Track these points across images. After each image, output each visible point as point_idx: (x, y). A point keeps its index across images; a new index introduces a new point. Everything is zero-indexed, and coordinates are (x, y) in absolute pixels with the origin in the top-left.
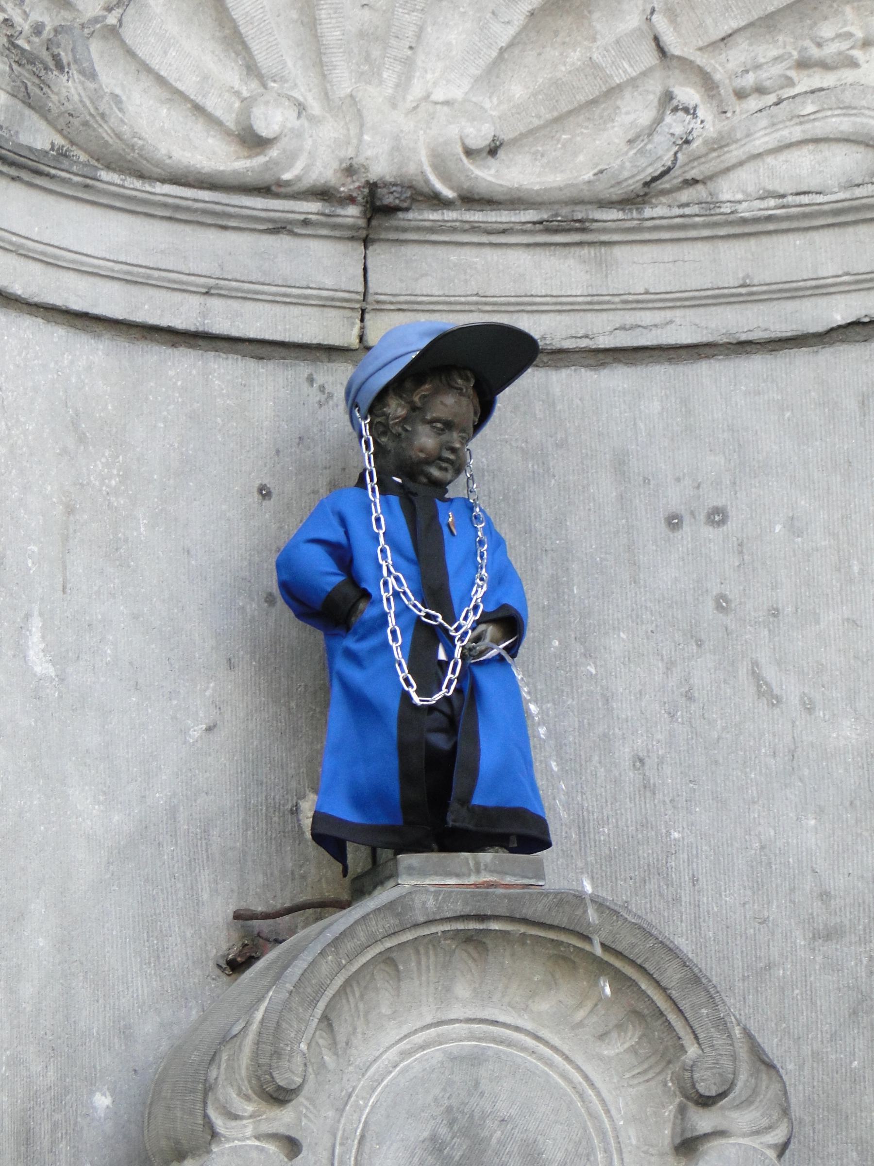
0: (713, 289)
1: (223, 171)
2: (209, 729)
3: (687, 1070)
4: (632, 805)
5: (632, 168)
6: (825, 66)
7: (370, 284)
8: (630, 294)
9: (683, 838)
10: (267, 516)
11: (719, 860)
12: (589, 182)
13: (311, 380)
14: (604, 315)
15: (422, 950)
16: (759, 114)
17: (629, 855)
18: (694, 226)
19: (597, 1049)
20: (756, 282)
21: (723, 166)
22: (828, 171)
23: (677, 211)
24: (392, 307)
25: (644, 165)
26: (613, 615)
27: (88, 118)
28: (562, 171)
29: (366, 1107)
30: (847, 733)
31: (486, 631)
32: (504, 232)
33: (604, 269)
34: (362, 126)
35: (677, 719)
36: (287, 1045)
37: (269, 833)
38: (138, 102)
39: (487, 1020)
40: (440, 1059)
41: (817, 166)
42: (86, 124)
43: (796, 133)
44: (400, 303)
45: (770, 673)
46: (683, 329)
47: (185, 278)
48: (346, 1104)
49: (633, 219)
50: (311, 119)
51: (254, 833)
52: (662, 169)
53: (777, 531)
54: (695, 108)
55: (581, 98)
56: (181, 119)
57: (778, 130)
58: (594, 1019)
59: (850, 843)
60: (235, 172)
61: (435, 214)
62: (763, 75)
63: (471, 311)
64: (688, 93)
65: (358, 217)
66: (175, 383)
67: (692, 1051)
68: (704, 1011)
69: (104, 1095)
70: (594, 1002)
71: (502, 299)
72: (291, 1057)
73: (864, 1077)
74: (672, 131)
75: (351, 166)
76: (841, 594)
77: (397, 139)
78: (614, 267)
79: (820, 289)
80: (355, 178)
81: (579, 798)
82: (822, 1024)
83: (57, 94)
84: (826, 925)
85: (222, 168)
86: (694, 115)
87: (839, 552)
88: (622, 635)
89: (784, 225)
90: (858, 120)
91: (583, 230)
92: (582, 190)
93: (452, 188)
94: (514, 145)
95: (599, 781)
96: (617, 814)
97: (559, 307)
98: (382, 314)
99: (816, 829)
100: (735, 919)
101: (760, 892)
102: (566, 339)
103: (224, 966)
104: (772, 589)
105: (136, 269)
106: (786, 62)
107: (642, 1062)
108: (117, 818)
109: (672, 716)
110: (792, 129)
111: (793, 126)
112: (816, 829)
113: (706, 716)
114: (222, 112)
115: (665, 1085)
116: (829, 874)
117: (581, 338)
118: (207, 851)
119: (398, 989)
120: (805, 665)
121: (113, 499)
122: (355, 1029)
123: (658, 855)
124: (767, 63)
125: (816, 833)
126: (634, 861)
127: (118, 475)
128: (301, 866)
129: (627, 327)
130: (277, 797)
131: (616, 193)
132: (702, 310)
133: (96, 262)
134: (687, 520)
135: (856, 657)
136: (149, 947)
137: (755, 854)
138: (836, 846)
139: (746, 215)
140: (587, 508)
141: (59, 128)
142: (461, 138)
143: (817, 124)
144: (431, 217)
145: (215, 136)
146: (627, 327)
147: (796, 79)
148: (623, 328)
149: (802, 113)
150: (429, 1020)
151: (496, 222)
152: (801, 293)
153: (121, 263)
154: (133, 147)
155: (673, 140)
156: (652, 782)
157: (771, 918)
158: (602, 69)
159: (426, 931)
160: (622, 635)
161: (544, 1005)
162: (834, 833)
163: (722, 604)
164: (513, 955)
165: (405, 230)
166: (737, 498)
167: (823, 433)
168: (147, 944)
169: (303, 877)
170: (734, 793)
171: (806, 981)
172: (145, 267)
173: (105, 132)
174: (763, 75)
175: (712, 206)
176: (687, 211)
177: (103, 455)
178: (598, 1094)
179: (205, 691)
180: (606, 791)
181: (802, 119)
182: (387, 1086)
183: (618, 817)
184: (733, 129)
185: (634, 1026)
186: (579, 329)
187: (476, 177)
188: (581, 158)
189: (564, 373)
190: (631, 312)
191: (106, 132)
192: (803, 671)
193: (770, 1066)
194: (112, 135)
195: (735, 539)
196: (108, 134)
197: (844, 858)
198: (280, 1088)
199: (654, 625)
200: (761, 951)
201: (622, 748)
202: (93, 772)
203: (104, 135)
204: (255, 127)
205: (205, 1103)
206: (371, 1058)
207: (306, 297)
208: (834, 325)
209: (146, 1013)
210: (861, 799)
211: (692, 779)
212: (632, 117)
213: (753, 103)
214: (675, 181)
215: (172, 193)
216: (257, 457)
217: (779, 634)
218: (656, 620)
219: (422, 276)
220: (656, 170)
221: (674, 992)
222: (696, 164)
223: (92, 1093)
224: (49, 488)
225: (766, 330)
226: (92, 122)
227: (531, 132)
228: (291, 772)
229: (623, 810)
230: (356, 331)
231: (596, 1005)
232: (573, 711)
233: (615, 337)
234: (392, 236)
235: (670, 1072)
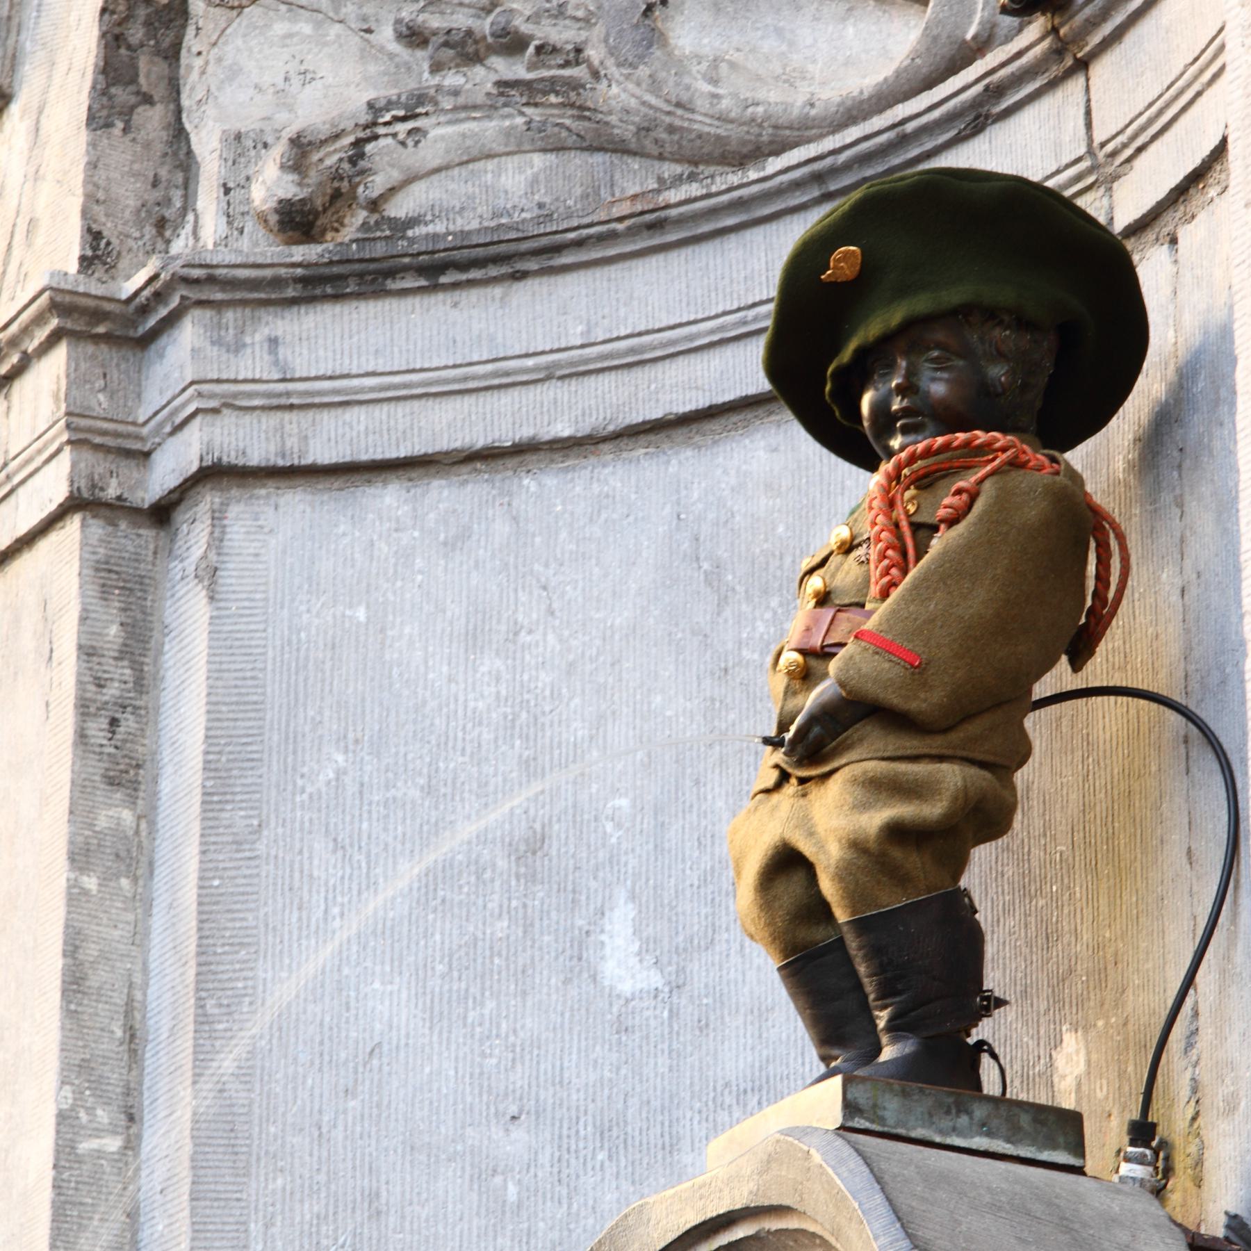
27: (668, 119)
38: (809, 41)
42: (671, 129)
56: (873, 28)
83: (610, 113)
141: (656, 153)
153: (754, 305)
173: (702, 124)
177: (768, 607)
203: (707, 129)
224: (659, 698)
226: (678, 122)
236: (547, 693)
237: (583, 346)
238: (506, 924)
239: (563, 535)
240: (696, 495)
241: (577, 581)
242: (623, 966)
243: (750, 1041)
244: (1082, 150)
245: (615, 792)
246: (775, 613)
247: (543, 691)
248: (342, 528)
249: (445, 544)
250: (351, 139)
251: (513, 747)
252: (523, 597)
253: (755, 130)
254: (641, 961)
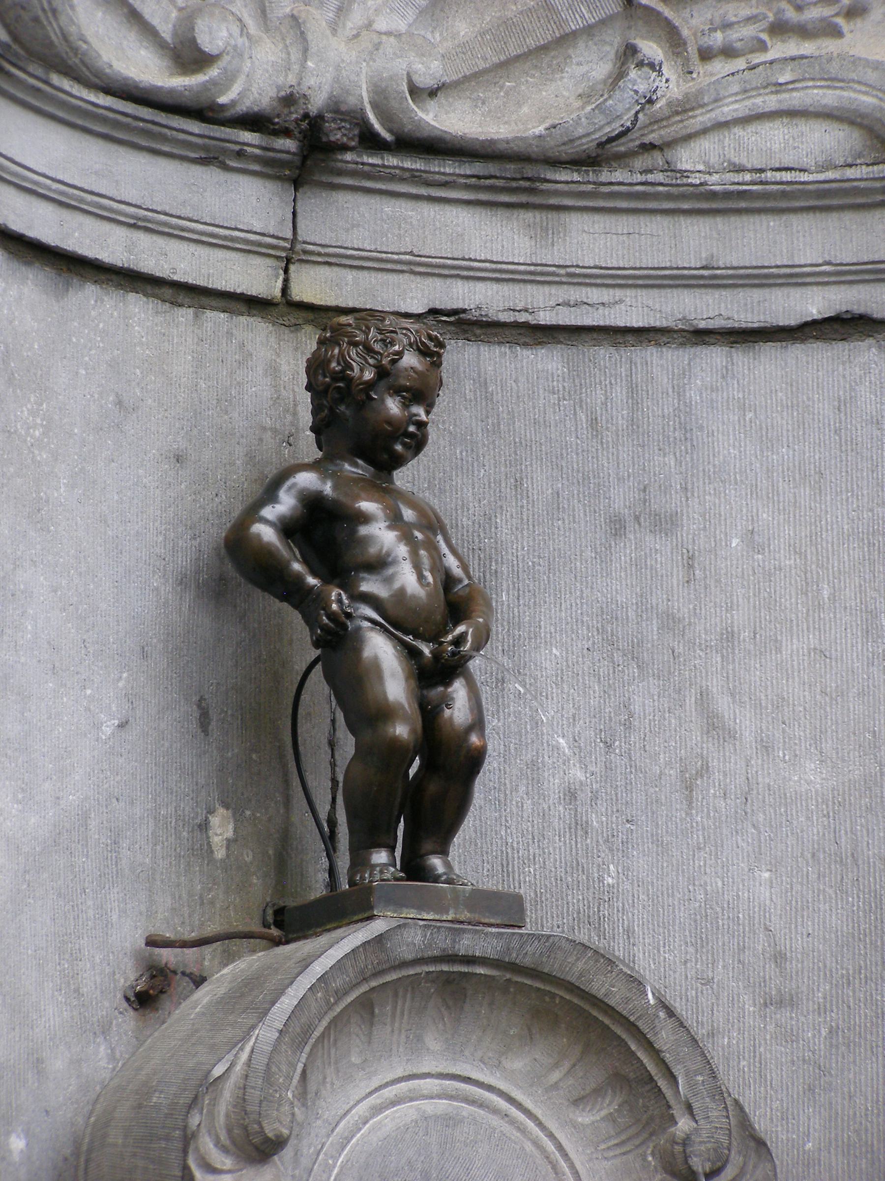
0: (671, 268)
1: (162, 87)
2: (122, 726)
3: (677, 1143)
4: (561, 844)
5: (585, 124)
6: (804, 32)
7: (299, 231)
8: (578, 266)
9: (618, 884)
10: (183, 486)
11: (658, 911)
12: (540, 136)
13: (230, 334)
14: (547, 289)
15: (401, 994)
16: (730, 78)
17: (557, 900)
18: (656, 196)
19: (571, 1116)
20: (721, 264)
21: (685, 132)
22: (810, 148)
23: (640, 178)
24: (320, 259)
25: (602, 123)
26: (545, 628)
27: (40, 13)
28: (506, 123)
29: (334, 1167)
30: (811, 776)
31: (466, 633)
32: (444, 185)
33: (550, 236)
34: (306, 50)
35: (615, 750)
36: (276, 1091)
37: (178, 850)
39: (460, 1076)
40: (414, 1117)
41: (791, 141)
42: (36, 20)
43: (771, 102)
45: (723, 704)
46: (633, 309)
48: (314, 1163)
49: (589, 182)
50: (249, 37)
51: (163, 848)
52: (621, 129)
53: (734, 545)
54: (660, 65)
55: (531, 43)
56: (115, 25)
57: (749, 97)
58: (571, 1081)
59: (810, 900)
60: (171, 91)
61: (375, 158)
62: (734, 35)
63: (402, 272)
64: (651, 49)
65: (294, 154)
66: (98, 325)
67: (684, 1124)
68: (700, 1078)
69: (18, 1136)
70: (572, 1063)
71: (438, 260)
72: (280, 1105)
73: (819, 1160)
74: (635, 88)
75: (292, 94)
76: (808, 622)
77: (339, 68)
78: (562, 235)
79: (793, 278)
80: (292, 109)
81: (503, 833)
82: (772, 1101)
84: (779, 991)
85: (160, 84)
86: (660, 73)
87: (805, 573)
88: (554, 651)
89: (758, 204)
90: (845, 94)
91: (532, 191)
92: (531, 145)
93: (390, 131)
94: (455, 87)
95: (525, 815)
96: (544, 853)
97: (498, 275)
98: (307, 266)
99: (771, 882)
100: (675, 978)
101: (704, 950)
102: (504, 310)
103: (133, 999)
104: (727, 610)
106: (761, 23)
107: (618, 1134)
108: (33, 820)
109: (609, 746)
110: (767, 98)
111: (767, 94)
112: (771, 882)
113: (647, 748)
114: (159, 20)
115: (644, 1159)
116: (785, 935)
117: (519, 311)
118: (117, 865)
119: (370, 1035)
120: (763, 697)
121: (36, 452)
122: (325, 1078)
123: (589, 902)
124: (739, 22)
125: (771, 887)
126: (563, 908)
127: (42, 425)
128: (210, 890)
129: (572, 303)
130: (187, 808)
131: (569, 151)
132: (656, 292)
134: (631, 525)
135: (823, 692)
136: (60, 971)
137: (700, 906)
138: (794, 902)
139: (717, 188)
140: (520, 504)
142: (408, 74)
143: (794, 94)
144: (370, 161)
145: (147, 48)
146: (572, 303)
147: (769, 44)
148: (567, 304)
149: (781, 80)
150: (399, 1073)
151: (439, 173)
152: (771, 281)
154: (76, 50)
155: (636, 97)
156: (584, 819)
157: (715, 980)
158: (557, 12)
159: (411, 972)
160: (554, 651)
161: (517, 1064)
162: (792, 888)
163: (670, 622)
164: (491, 1004)
165: (340, 173)
166: (688, 506)
167: (791, 439)
168: (58, 967)
169: (212, 903)
170: (677, 837)
171: (755, 1052)
174: (734, 35)
175: (679, 175)
176: (650, 177)
177: (29, 400)
178: (572, 1166)
179: (118, 681)
180: (533, 826)
181: (779, 88)
182: (357, 1144)
183: (546, 856)
184: (700, 92)
185: (614, 1092)
186: (517, 301)
187: (421, 119)
188: (525, 109)
189: (497, 350)
190: (577, 288)
191: (54, 29)
192: (761, 704)
193: (761, 1144)
194: (59, 34)
195: (685, 551)
196: (55, 33)
197: (803, 917)
198: (267, 1140)
199: (590, 642)
200: (703, 1016)
201: (551, 779)
202: (13, 765)
204: (199, 41)
205: (185, 1152)
206: (341, 1112)
208: (809, 319)
209: (57, 1047)
210: (825, 852)
211: (629, 818)
212: (584, 69)
213: (720, 67)
214: (631, 145)
215: (115, 107)
216: (174, 417)
217: (734, 660)
218: (593, 636)
219: (353, 226)
220: (613, 130)
221: (668, 1055)
222: (656, 127)
223: (8, 1134)
225: (729, 318)
227: (476, 75)
228: (202, 781)
229: (551, 849)
230: (279, 284)
231: (574, 1065)
232: (498, 734)
233: (557, 314)
234: (325, 178)
235: (651, 1145)
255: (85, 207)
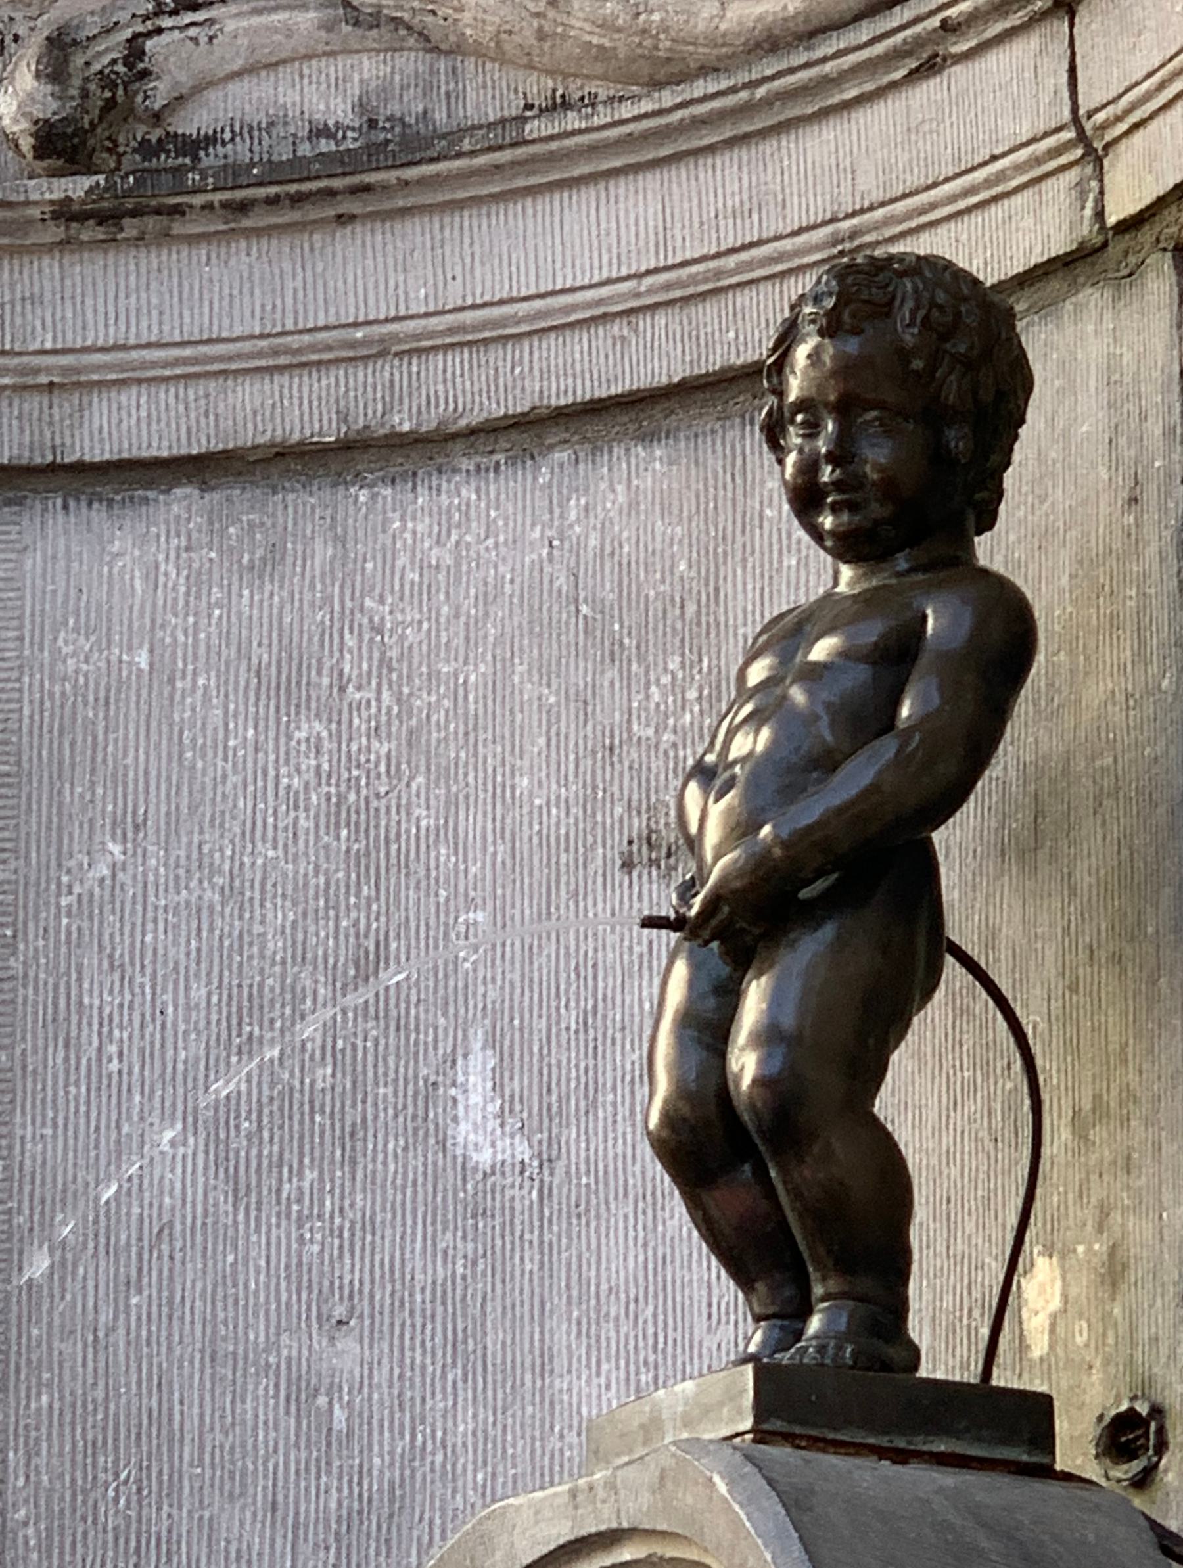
24: (1123, 127)
44: (1127, 112)
47: (787, 245)
105: (684, 273)
133: (589, 295)
153: (649, 272)
172: (704, 258)
177: (666, 669)
203: (588, 38)
207: (1001, 177)
236: (383, 768)
237: (427, 315)
238: (329, 1071)
239: (402, 560)
240: (573, 515)
241: (420, 622)
242: (480, 1131)
243: (641, 1234)
244: (1067, 115)
245: (471, 904)
246: (674, 678)
247: (377, 765)
248: (116, 546)
249: (252, 568)
250: (128, 33)
251: (338, 838)
252: (350, 641)
253: (648, 43)
254: (502, 1125)
255: (734, 280)
